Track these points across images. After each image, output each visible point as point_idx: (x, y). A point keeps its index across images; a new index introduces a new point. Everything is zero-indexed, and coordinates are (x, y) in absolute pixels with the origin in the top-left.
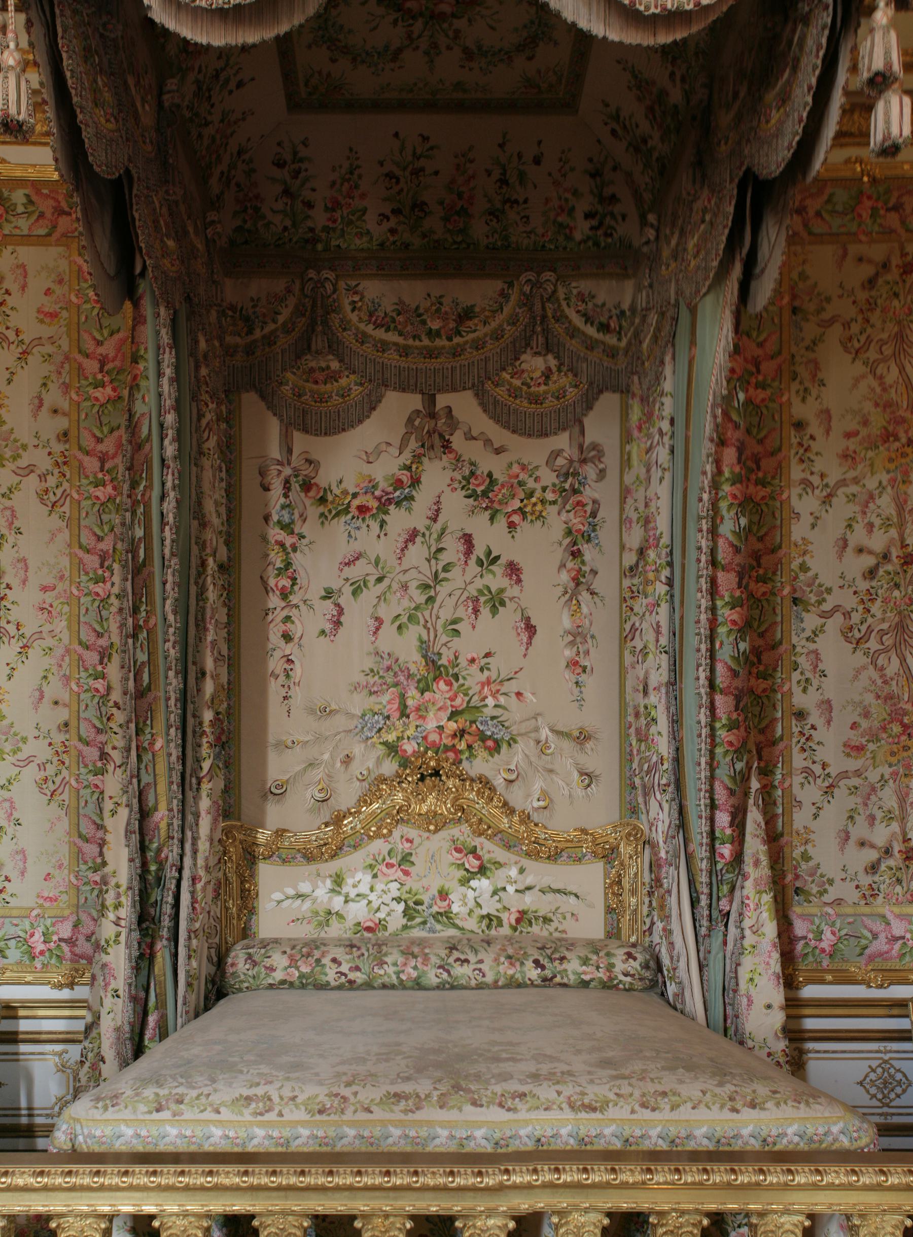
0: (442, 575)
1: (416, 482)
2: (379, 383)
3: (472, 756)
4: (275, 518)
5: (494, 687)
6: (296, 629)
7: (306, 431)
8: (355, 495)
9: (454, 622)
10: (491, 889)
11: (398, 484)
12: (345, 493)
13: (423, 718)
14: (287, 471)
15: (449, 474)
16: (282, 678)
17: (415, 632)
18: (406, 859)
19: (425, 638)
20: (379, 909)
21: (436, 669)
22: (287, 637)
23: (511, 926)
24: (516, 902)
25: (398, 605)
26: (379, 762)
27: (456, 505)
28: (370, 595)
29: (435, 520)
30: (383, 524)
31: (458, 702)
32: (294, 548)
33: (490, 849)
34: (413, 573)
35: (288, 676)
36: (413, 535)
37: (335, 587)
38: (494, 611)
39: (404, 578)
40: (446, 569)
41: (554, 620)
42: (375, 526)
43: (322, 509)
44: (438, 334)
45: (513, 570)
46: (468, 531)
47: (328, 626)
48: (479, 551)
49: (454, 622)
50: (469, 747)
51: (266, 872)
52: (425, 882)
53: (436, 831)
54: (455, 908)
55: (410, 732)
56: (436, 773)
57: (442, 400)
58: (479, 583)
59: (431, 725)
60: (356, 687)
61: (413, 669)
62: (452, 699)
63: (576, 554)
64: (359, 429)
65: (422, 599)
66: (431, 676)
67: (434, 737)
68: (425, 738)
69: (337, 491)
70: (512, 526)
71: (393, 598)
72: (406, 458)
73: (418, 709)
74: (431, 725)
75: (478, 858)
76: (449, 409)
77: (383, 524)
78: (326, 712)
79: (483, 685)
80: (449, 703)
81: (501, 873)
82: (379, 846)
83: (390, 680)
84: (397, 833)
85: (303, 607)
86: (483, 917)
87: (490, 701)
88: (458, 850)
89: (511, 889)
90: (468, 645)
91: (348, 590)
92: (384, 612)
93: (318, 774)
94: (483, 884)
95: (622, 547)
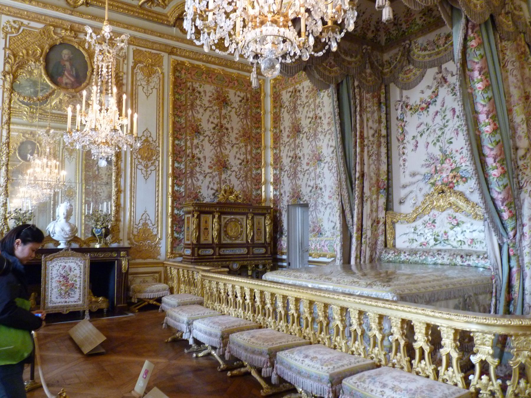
0: (446, 124)
1: (437, 96)
2: (425, 67)
3: (458, 184)
4: (399, 118)
5: (464, 159)
6: (406, 151)
7: (406, 89)
8: (420, 105)
9: (451, 139)
10: (461, 231)
12: (417, 105)
13: (442, 173)
14: (401, 103)
15: (447, 89)
16: (402, 166)
17: (438, 144)
18: (434, 222)
19: (442, 146)
20: (426, 239)
21: (446, 156)
22: (404, 154)
23: (469, 245)
24: (468, 235)
25: (433, 137)
26: (430, 189)
28: (425, 136)
29: (443, 106)
31: (453, 166)
32: (404, 126)
33: (460, 217)
34: (437, 126)
35: (404, 165)
36: (437, 113)
37: (415, 135)
39: (434, 128)
40: (447, 122)
43: (411, 112)
46: (453, 107)
47: (414, 148)
49: (451, 139)
50: (457, 181)
51: (398, 226)
52: (440, 229)
53: (442, 212)
54: (449, 238)
55: (438, 179)
56: (443, 192)
57: (444, 66)
59: (444, 175)
60: (422, 166)
61: (439, 157)
62: (451, 165)
64: (420, 84)
65: (439, 133)
66: (444, 159)
67: (446, 179)
68: (443, 180)
69: (414, 105)
71: (432, 135)
73: (440, 170)
74: (444, 175)
75: (457, 220)
76: (446, 68)
77: (428, 111)
78: (414, 175)
79: (461, 159)
80: (450, 167)
81: (465, 225)
82: (426, 218)
83: (432, 162)
84: (431, 213)
85: (407, 143)
86: (458, 241)
87: (463, 164)
88: (450, 218)
89: (468, 231)
91: (419, 135)
93: (412, 195)
94: (458, 229)
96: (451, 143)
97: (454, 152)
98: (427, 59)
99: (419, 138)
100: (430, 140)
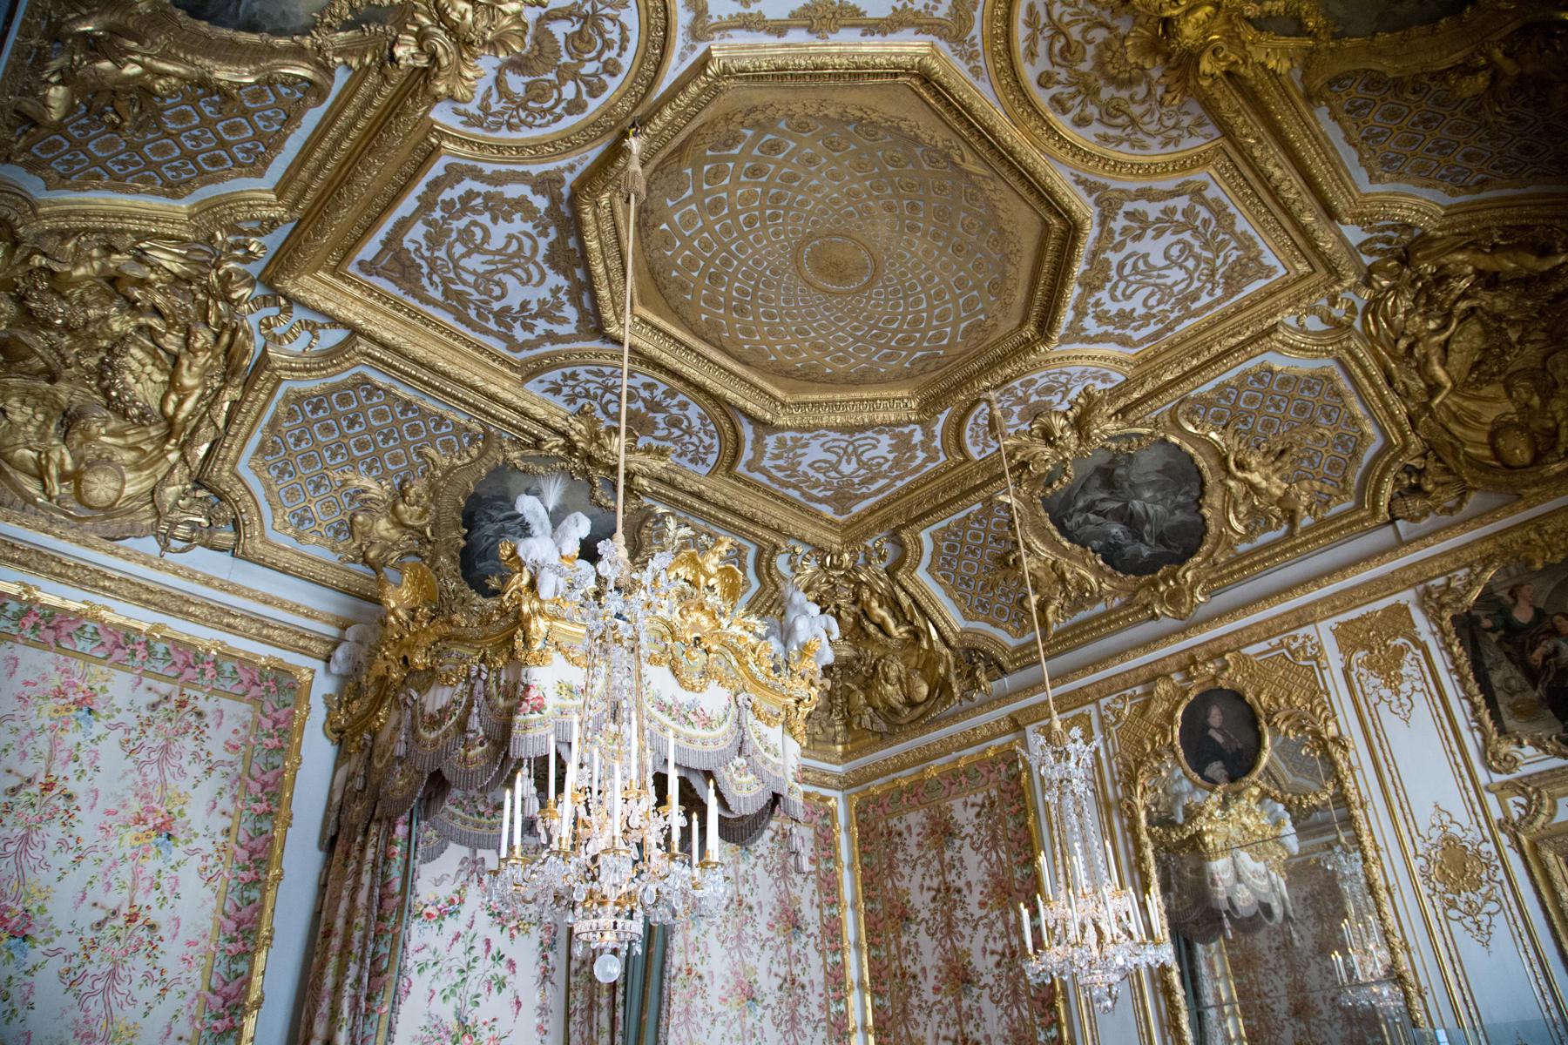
1: (462, 902)
9: (478, 996)
11: (452, 902)
15: (480, 900)
17: (453, 1000)
25: (444, 983)
27: (483, 919)
28: (429, 972)
30: (440, 927)
36: (458, 936)
38: (499, 990)
41: (532, 997)
42: (436, 927)
44: (481, 814)
45: (511, 964)
48: (493, 951)
49: (478, 996)
57: (481, 853)
58: (492, 972)
63: (545, 958)
70: (512, 936)
71: (442, 977)
72: (457, 886)
77: (440, 927)
90: (480, 1015)
91: (416, 969)
92: (437, 987)
95: (569, 958)
96: (477, 1004)
97: (479, 1023)
98: (457, 822)
99: (414, 976)
100: (437, 987)
